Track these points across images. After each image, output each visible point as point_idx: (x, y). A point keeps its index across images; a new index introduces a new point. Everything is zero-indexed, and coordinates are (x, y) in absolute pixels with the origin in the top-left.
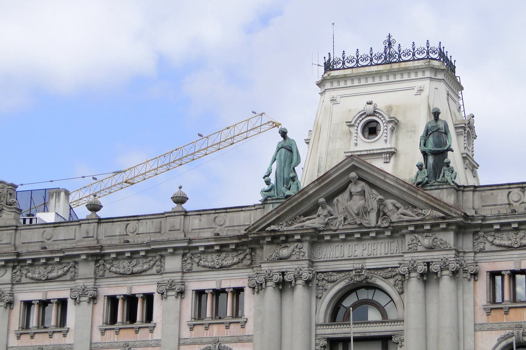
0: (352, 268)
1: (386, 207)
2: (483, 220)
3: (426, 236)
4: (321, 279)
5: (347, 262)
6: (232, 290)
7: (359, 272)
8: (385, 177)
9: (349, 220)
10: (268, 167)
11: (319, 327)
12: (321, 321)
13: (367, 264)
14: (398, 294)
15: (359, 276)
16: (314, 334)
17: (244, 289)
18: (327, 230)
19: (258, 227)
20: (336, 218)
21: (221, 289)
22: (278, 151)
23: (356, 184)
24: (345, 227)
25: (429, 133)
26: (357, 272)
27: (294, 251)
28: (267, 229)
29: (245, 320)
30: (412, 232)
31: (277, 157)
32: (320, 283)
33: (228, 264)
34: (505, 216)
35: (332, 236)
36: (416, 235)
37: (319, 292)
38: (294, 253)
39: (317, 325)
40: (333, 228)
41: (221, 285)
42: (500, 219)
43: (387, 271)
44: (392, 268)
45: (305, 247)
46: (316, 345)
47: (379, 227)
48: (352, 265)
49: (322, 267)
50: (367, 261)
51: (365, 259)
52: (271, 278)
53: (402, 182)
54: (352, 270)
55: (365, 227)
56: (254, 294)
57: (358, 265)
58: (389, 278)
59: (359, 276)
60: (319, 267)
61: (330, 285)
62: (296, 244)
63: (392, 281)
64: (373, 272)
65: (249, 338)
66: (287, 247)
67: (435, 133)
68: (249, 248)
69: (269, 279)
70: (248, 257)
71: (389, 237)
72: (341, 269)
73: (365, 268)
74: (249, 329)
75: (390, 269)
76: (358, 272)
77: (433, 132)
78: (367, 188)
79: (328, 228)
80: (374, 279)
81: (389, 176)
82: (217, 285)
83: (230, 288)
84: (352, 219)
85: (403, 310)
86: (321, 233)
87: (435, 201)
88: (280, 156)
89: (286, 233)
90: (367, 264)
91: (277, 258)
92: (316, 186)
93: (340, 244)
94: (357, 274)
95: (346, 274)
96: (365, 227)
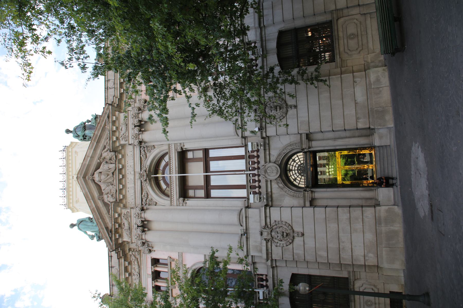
0: (140, 181)
1: (106, 157)
2: (117, 98)
3: (121, 130)
4: (145, 202)
5: (136, 184)
6: (153, 267)
7: (141, 175)
8: (88, 156)
9: (111, 180)
10: (88, 236)
11: (173, 204)
12: (169, 202)
13: (138, 171)
14: (155, 149)
15: (143, 176)
16: (176, 207)
17: (153, 258)
18: (116, 196)
19: (110, 242)
20: (111, 190)
21: (152, 274)
22: (81, 230)
23: (94, 178)
24: (115, 184)
25: (78, 136)
26: (141, 177)
27: (126, 219)
28: (110, 236)
29: (169, 258)
30: (117, 138)
31: (85, 230)
32: (148, 203)
33: (138, 268)
34: (116, 84)
35: (120, 193)
36: (120, 136)
37: (152, 203)
38: (127, 219)
39: (171, 205)
40: (115, 192)
41: (149, 275)
42: (117, 87)
43: (142, 158)
44: (140, 154)
45: (124, 211)
46: (183, 205)
47: (116, 161)
48: (138, 181)
49: (139, 201)
50: (136, 171)
51: (135, 172)
52: (140, 236)
53: (91, 145)
54: (141, 181)
55: (115, 170)
56: (155, 251)
57: (137, 176)
58: (146, 156)
59: (143, 176)
60: (139, 204)
61: (149, 197)
62: (122, 217)
63: (148, 155)
64: (142, 167)
65: (180, 255)
66: (124, 224)
67: (76, 131)
68: (129, 252)
69: (140, 237)
70: (134, 253)
71: (123, 156)
72: (140, 188)
73: (140, 172)
74: (175, 256)
75: (141, 156)
76: (141, 176)
77: (75, 132)
78: (99, 171)
79: (114, 196)
80: (147, 167)
81: (88, 154)
82: (150, 277)
83: (152, 268)
84: (110, 179)
85: (164, 145)
86: (118, 200)
87: (100, 123)
88: (84, 228)
89: (113, 223)
90: (138, 171)
91: (129, 231)
92: (90, 202)
93: (128, 189)
94: (142, 177)
95: (143, 184)
96: (115, 170)
